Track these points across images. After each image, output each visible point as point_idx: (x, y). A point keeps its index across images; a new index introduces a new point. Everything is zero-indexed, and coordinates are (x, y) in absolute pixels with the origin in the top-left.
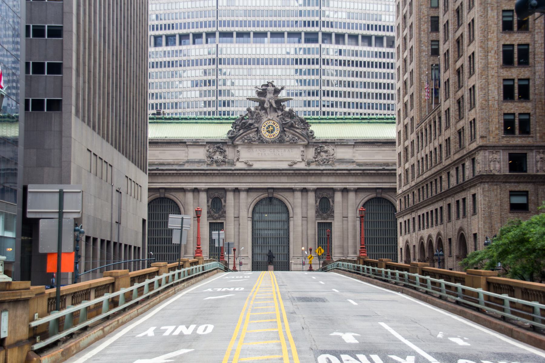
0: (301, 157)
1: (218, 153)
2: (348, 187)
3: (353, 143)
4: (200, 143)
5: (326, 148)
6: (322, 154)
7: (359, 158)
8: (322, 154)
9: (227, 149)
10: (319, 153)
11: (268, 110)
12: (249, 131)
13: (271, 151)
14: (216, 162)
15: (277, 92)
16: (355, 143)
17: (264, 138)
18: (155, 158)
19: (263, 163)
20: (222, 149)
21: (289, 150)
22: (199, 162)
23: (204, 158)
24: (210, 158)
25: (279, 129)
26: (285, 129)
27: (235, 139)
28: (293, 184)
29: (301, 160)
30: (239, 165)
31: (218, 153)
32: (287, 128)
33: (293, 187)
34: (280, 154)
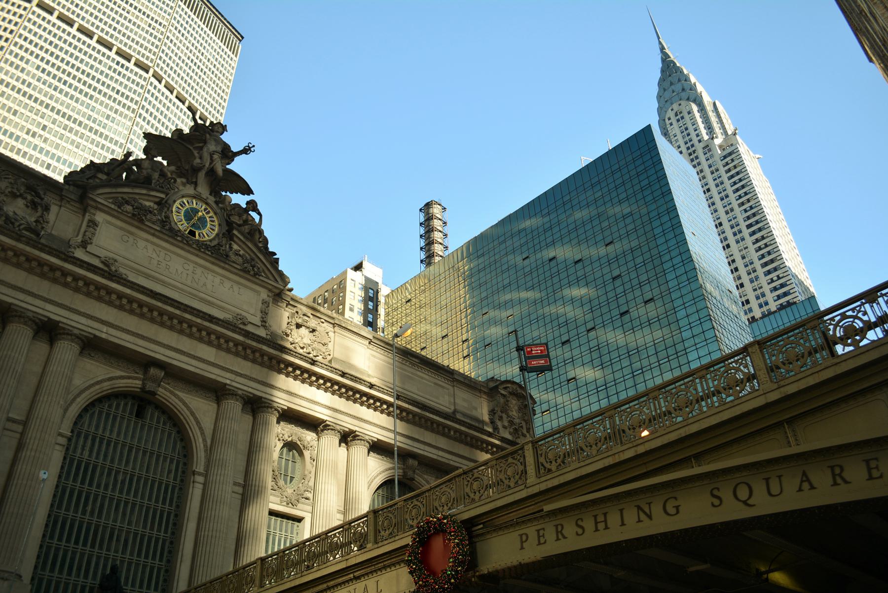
0: (259, 315)
5: (313, 323)
6: (303, 330)
9: (54, 209)
10: (298, 326)
11: (202, 175)
12: (144, 192)
13: (186, 266)
15: (228, 155)
21: (232, 287)
26: (235, 232)
28: (228, 375)
29: (259, 324)
31: (20, 202)
32: (240, 232)
33: (228, 382)
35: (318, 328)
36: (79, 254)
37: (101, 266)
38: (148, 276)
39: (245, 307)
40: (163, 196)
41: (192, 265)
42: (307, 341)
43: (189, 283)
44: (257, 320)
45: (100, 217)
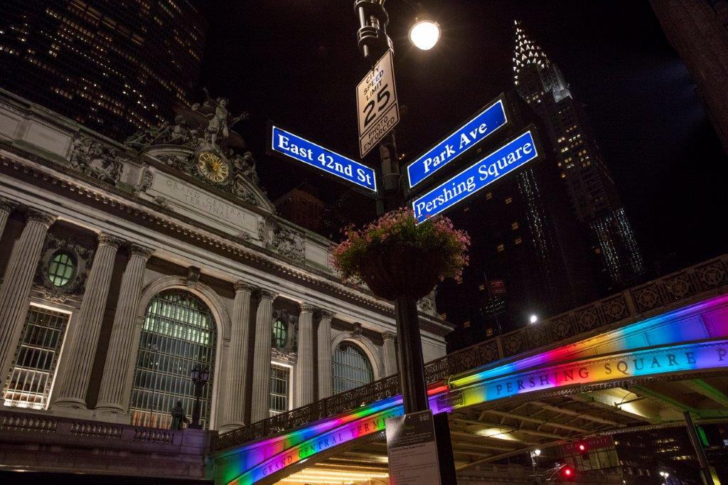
8: (288, 243)
12: (180, 150)
24: (80, 162)
25: (227, 173)
34: (224, 213)
35: (295, 240)
36: (142, 195)
37: (156, 203)
38: (185, 208)
39: (248, 228)
40: (191, 152)
42: (288, 249)
43: (212, 212)
44: (256, 236)
45: (152, 169)
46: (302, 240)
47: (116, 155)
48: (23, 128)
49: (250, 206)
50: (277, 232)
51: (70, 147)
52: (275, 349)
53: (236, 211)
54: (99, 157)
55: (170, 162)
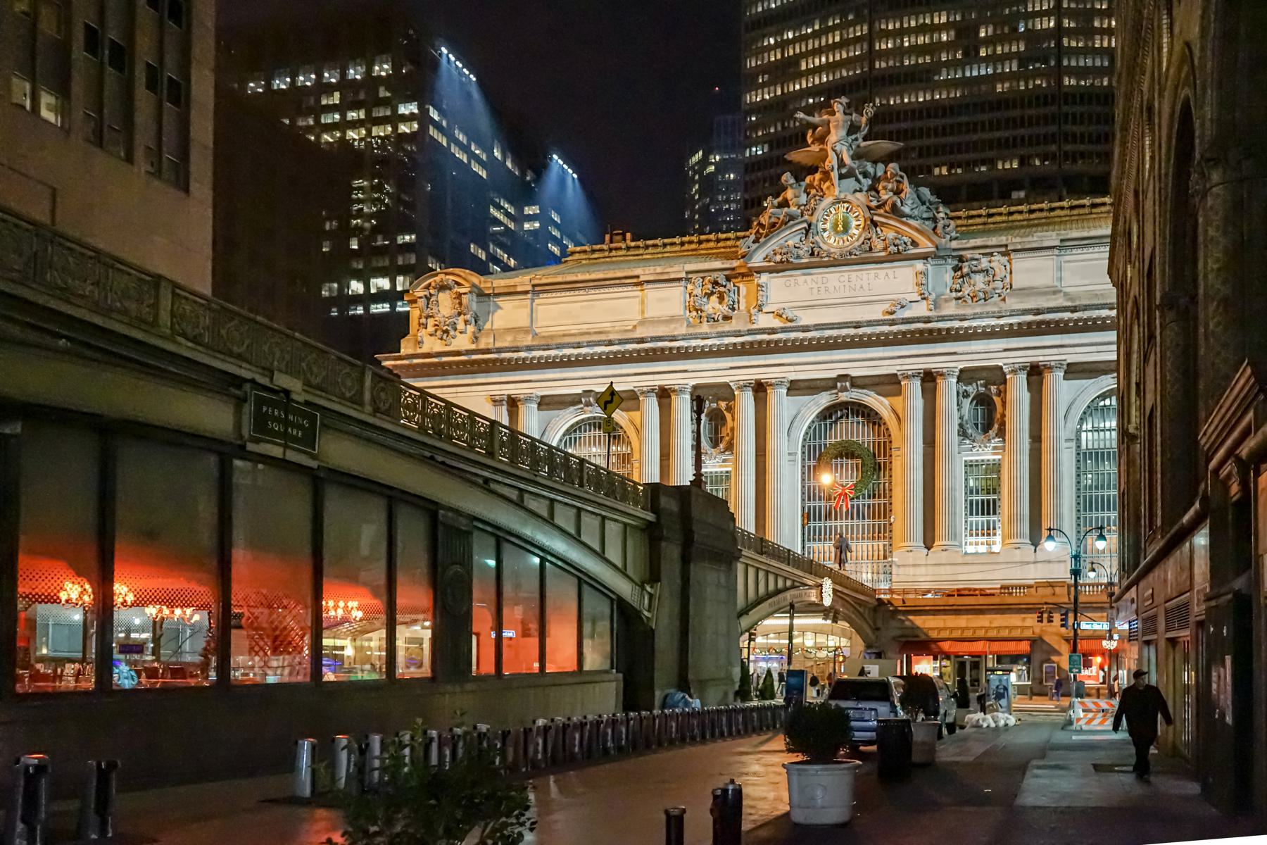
1: (714, 298)
2: (1041, 359)
3: (1057, 243)
4: (672, 276)
7: (1073, 283)
13: (842, 279)
14: (711, 319)
16: (1062, 241)
17: (825, 247)
18: (570, 322)
19: (824, 311)
20: (725, 286)
22: (672, 320)
23: (682, 313)
24: (697, 310)
25: (862, 222)
27: (751, 258)
29: (919, 298)
30: (764, 321)
31: (714, 298)
34: (866, 287)
35: (993, 265)
41: (846, 274)
42: (980, 286)
43: (847, 294)
45: (764, 278)
46: (1004, 260)
47: (728, 279)
48: (643, 302)
49: (897, 256)
50: (956, 269)
51: (685, 297)
52: (968, 442)
53: (882, 273)
54: (712, 293)
55: (778, 258)
